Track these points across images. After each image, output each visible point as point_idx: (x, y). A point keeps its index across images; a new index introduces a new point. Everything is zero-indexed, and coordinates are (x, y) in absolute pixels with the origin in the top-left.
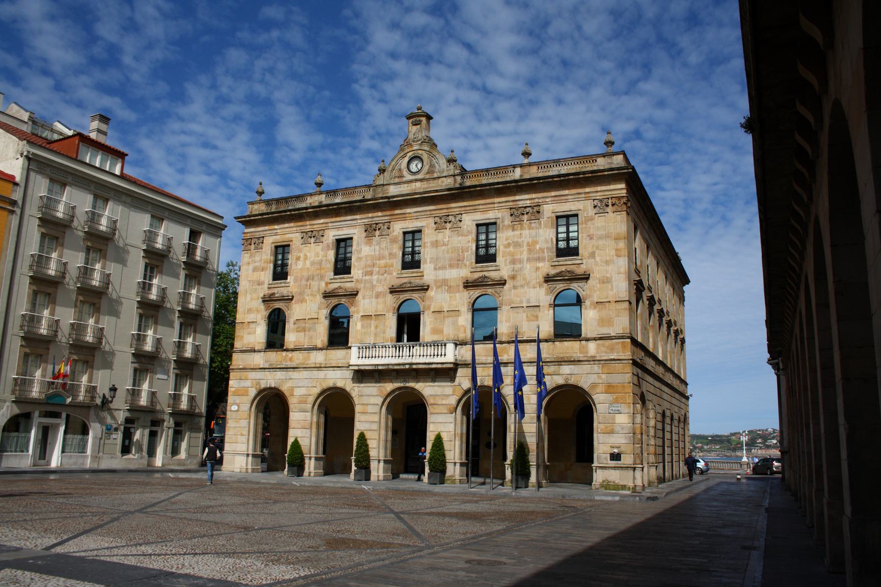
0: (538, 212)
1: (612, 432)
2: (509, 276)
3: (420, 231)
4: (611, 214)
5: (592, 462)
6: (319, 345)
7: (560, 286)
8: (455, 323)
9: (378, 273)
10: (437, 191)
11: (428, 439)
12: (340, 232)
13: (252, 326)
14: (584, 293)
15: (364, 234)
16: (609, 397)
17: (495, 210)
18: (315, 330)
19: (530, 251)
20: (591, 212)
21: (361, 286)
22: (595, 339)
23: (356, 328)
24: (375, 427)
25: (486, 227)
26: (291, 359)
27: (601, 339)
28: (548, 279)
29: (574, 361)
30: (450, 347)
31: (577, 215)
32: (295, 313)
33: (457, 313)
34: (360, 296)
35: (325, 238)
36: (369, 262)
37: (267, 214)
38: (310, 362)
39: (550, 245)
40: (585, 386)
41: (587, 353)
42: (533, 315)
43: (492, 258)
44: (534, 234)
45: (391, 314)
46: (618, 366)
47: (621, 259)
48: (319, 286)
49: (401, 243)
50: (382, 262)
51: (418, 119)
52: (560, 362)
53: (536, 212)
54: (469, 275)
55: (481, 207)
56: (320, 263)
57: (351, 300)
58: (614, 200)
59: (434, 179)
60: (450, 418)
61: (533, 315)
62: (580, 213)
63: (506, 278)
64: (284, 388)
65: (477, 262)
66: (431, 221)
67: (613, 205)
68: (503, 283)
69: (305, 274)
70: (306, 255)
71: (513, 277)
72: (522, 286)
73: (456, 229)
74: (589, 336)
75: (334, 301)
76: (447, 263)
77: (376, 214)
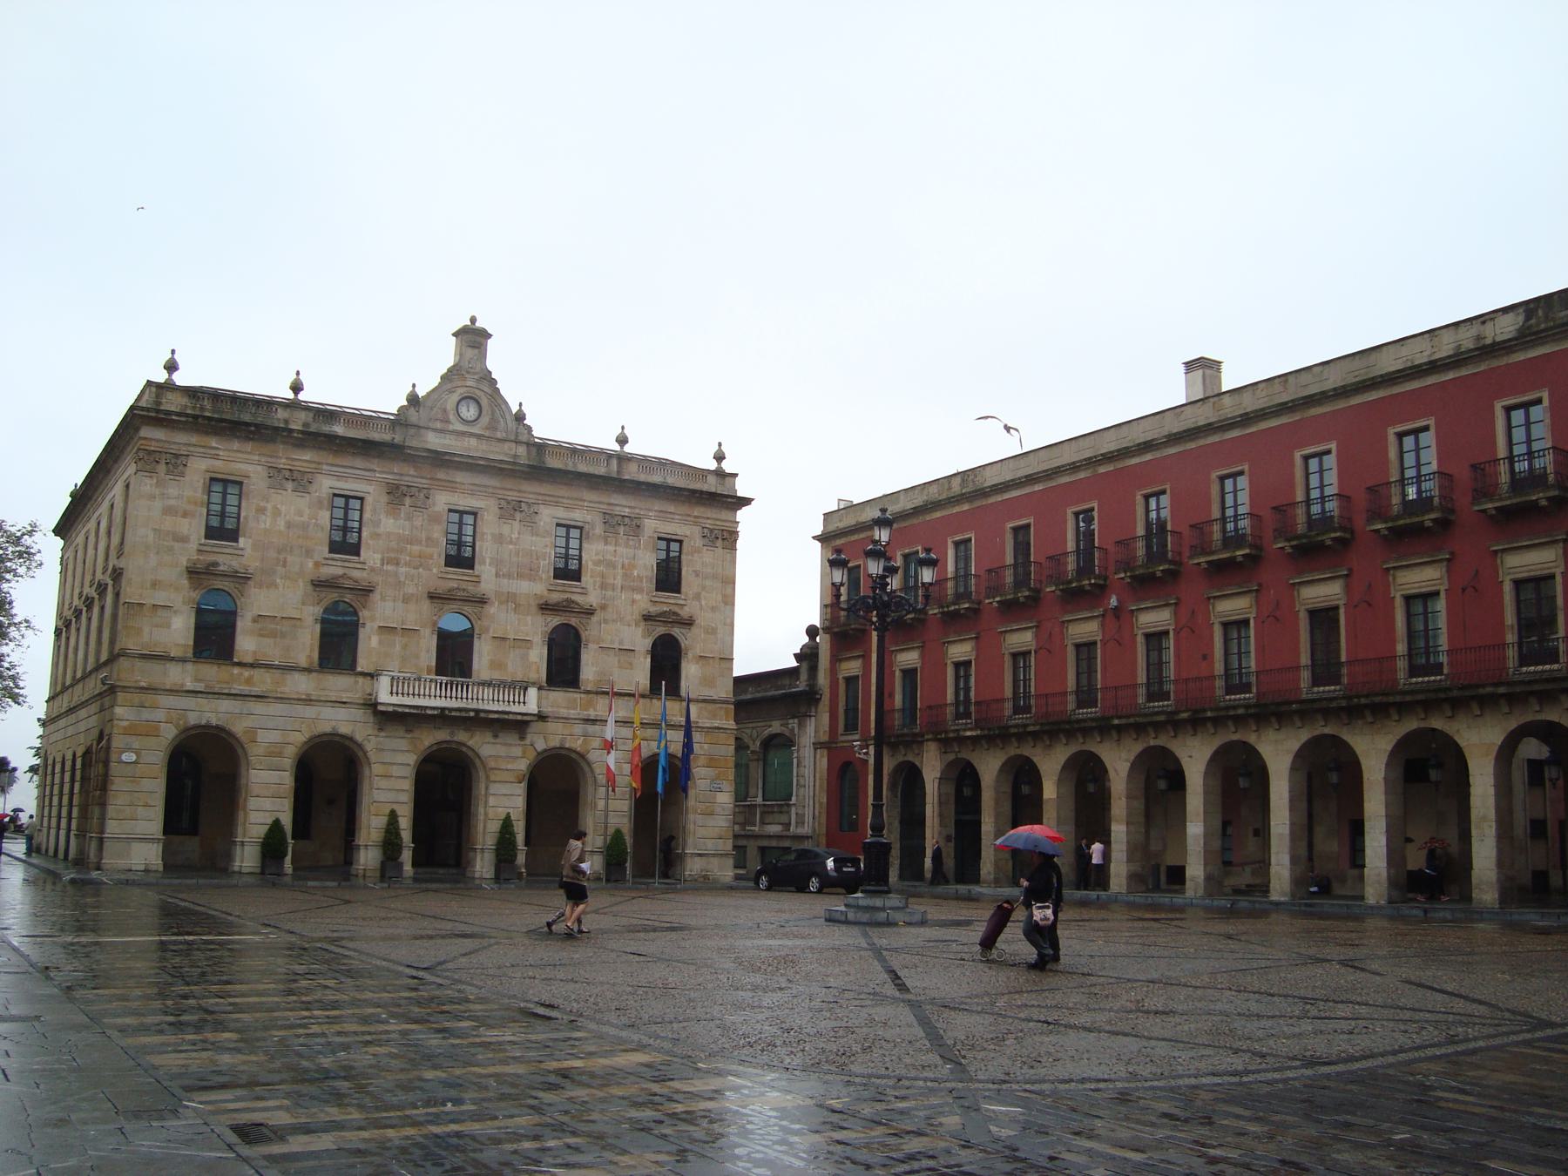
4: (720, 550)
6: (303, 663)
8: (525, 657)
9: (407, 564)
13: (160, 612)
15: (384, 499)
17: (585, 509)
19: (625, 575)
20: (699, 542)
23: (370, 644)
28: (647, 618)
30: (532, 692)
31: (681, 542)
32: (256, 603)
34: (376, 596)
35: (312, 488)
36: (393, 544)
38: (287, 690)
50: (416, 548)
53: (636, 528)
56: (305, 527)
59: (499, 440)
64: (238, 728)
68: (590, 612)
70: (275, 507)
71: (604, 607)
73: (530, 522)
75: (333, 596)
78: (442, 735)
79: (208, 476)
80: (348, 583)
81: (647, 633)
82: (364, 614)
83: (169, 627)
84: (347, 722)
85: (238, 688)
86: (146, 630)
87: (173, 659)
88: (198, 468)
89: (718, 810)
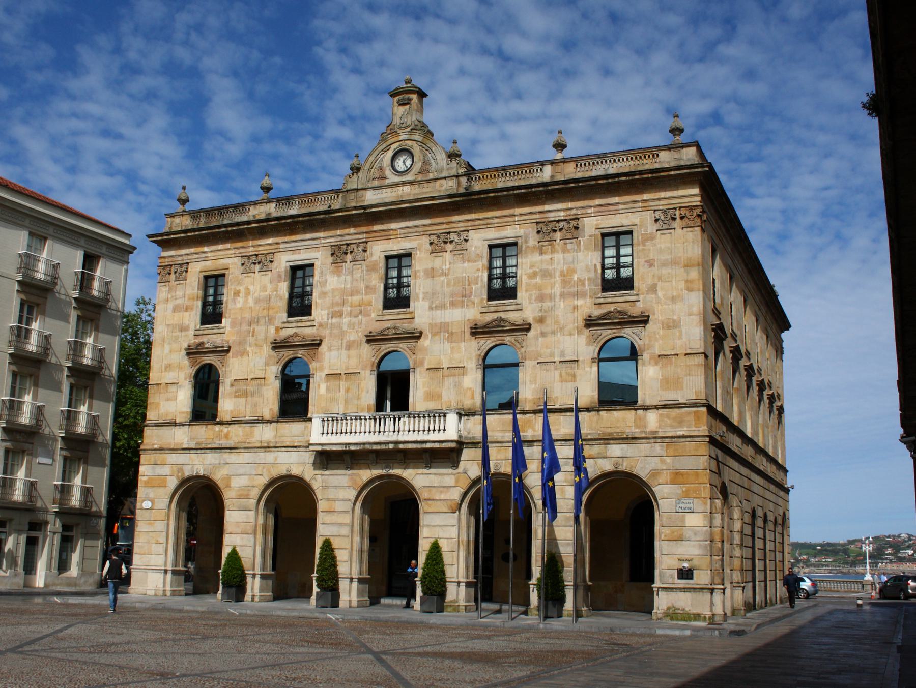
0: (576, 228)
1: (680, 539)
2: (534, 319)
3: (409, 255)
4: (679, 231)
5: (653, 582)
6: (267, 416)
7: (608, 333)
8: (459, 385)
9: (350, 314)
10: (433, 198)
11: (420, 549)
12: (297, 257)
13: (172, 389)
14: (640, 342)
15: (330, 259)
16: (676, 489)
17: (516, 225)
18: (261, 395)
19: (565, 282)
20: (651, 228)
22: (656, 408)
24: (345, 531)
25: (503, 249)
26: (227, 436)
27: (664, 407)
28: (590, 323)
29: (627, 439)
30: (452, 418)
31: (630, 233)
32: (232, 370)
33: (462, 370)
34: (324, 347)
35: (275, 264)
36: (337, 299)
37: (194, 230)
38: (253, 440)
39: (592, 275)
40: (643, 474)
41: (645, 426)
42: (569, 374)
44: (571, 259)
45: (368, 372)
46: (689, 446)
47: (693, 293)
48: (266, 331)
49: (382, 271)
50: (356, 299)
51: (407, 96)
52: (607, 440)
53: (573, 227)
54: (479, 317)
55: (495, 221)
57: (311, 352)
58: (683, 212)
59: (429, 181)
60: (452, 519)
61: (569, 374)
62: (635, 229)
63: (531, 321)
64: (218, 477)
65: (490, 298)
66: (425, 240)
67: (682, 218)
68: (525, 328)
69: (247, 316)
71: (541, 320)
72: (553, 332)
73: (460, 251)
75: (288, 354)
76: (447, 300)
77: (346, 231)
79: (202, 275)
80: (298, 341)
81: (593, 340)
82: (313, 366)
83: (176, 399)
86: (162, 403)
87: (175, 424)
88: (196, 271)
89: (688, 534)
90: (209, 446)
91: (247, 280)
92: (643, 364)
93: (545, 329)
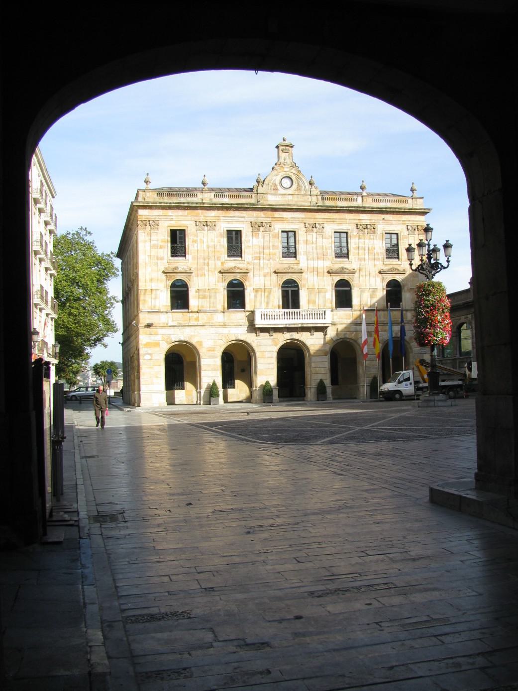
8: (324, 297)
17: (347, 222)
20: (406, 233)
21: (250, 267)
26: (197, 319)
34: (250, 275)
43: (347, 256)
45: (277, 289)
50: (267, 251)
55: (337, 220)
64: (194, 341)
70: (201, 240)
71: (360, 270)
74: (407, 308)
78: (288, 336)
79: (169, 229)
82: (246, 284)
84: (241, 333)
85: (192, 323)
86: (149, 300)
90: (187, 325)
91: (200, 234)
92: (405, 292)
93: (363, 273)
